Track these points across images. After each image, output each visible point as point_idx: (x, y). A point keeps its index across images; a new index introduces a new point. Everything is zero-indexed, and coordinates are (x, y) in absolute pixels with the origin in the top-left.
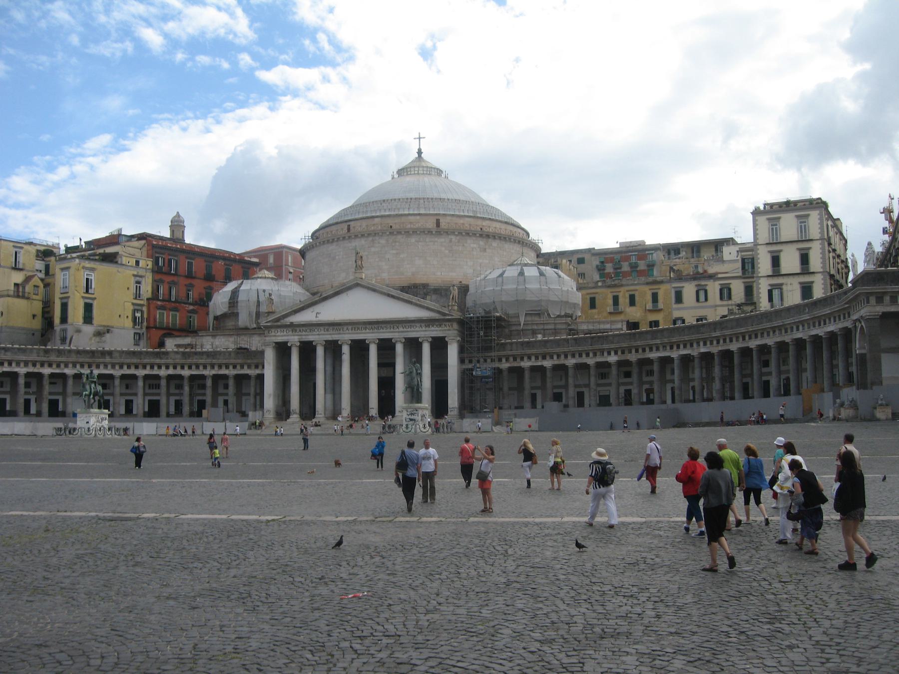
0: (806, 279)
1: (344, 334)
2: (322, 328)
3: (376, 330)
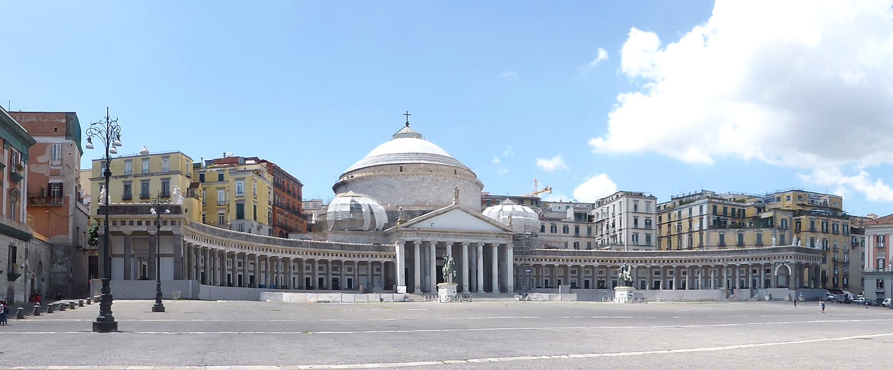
0: (648, 232)
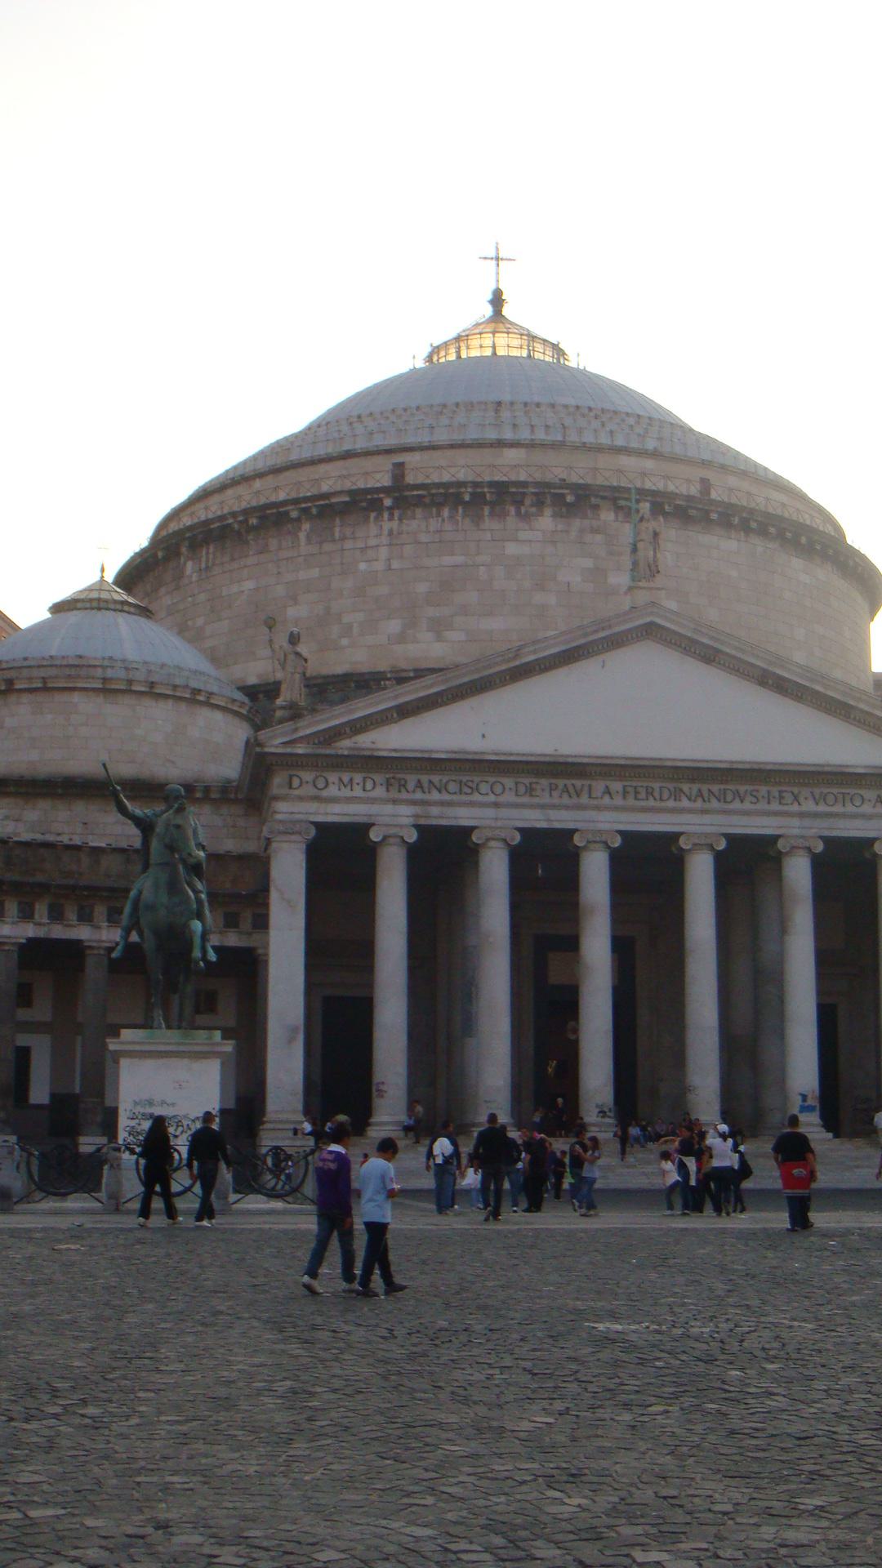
1: (598, 808)
2: (509, 782)
3: (715, 804)
